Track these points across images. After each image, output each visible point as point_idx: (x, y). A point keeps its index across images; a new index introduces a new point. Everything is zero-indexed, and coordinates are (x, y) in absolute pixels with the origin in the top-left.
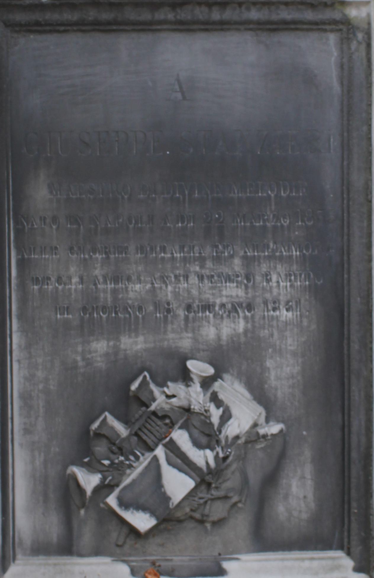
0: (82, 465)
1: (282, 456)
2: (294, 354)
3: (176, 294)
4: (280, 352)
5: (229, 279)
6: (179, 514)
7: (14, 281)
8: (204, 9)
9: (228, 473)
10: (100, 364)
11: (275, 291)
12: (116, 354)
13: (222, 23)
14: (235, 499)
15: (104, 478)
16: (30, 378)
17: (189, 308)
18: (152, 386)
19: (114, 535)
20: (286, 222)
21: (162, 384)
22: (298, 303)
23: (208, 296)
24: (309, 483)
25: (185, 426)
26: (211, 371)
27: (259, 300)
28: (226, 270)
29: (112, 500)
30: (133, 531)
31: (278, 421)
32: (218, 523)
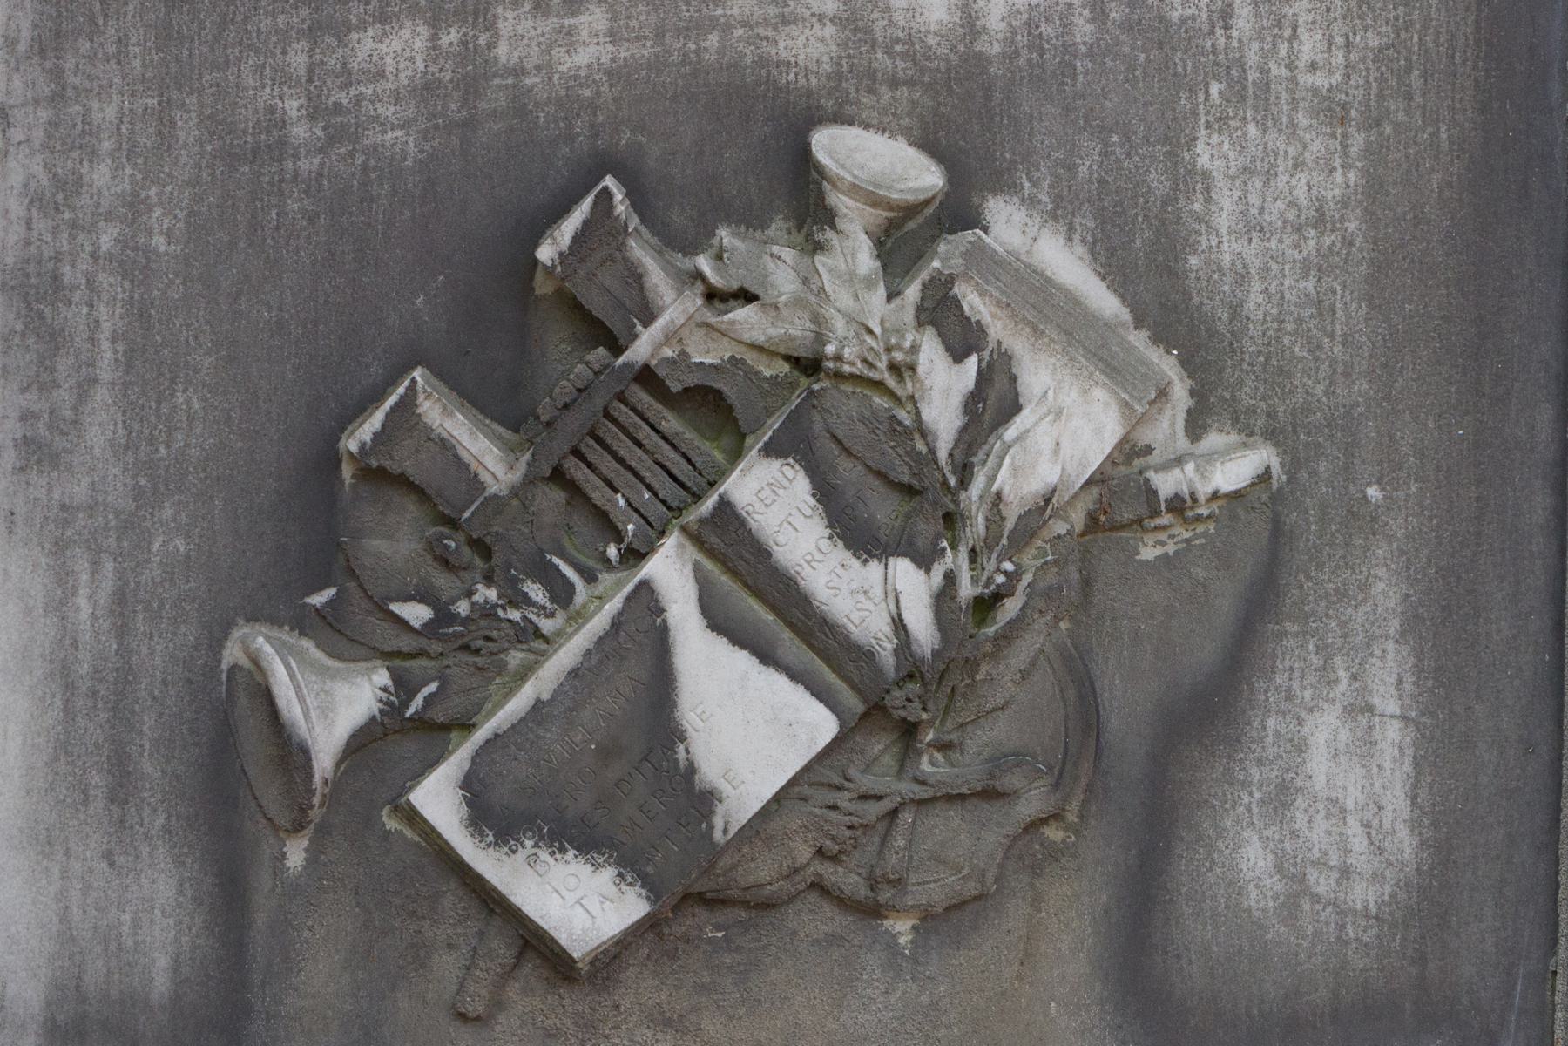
0: (305, 623)
2: (1333, 112)
6: (762, 870)
12: (471, 87)
14: (1032, 803)
15: (404, 686)
18: (641, 252)
19: (447, 966)
24: (1392, 734)
31: (1246, 428)
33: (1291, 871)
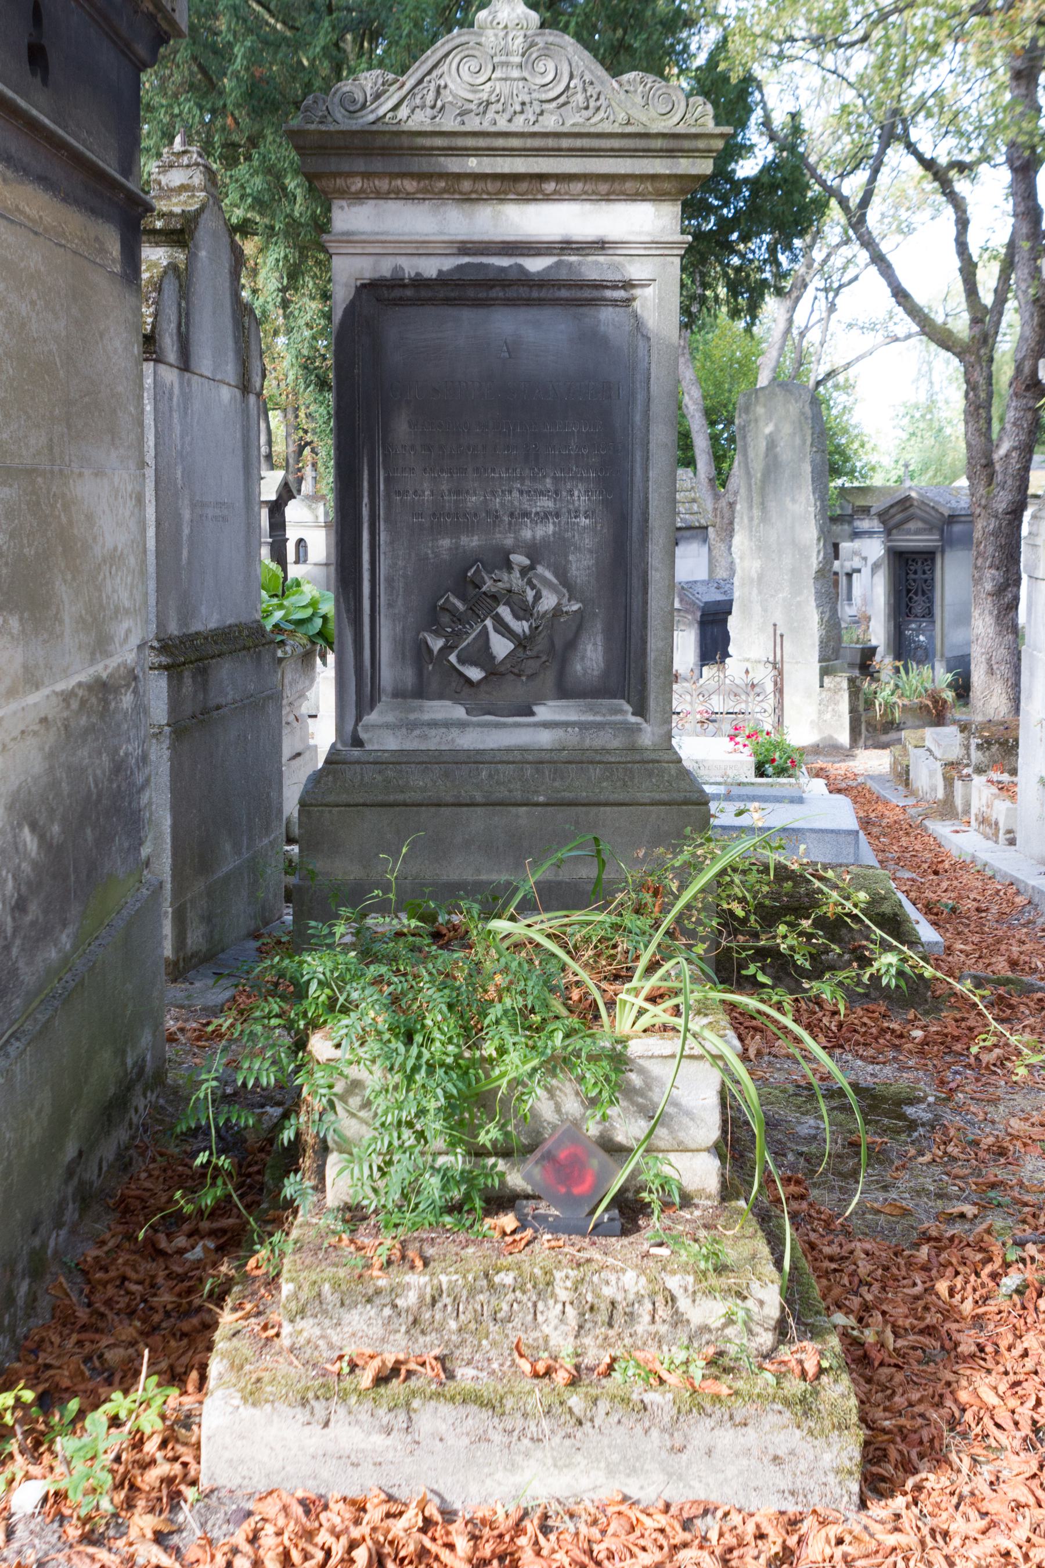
1: (580, 628)
2: (590, 551)
3: (502, 504)
4: (578, 549)
5: (542, 493)
6: (502, 669)
7: (382, 493)
8: (526, 289)
9: (539, 639)
10: (445, 556)
11: (577, 503)
12: (457, 548)
13: (540, 299)
14: (544, 659)
15: (447, 641)
16: (393, 566)
17: (512, 515)
18: (484, 574)
19: (454, 684)
20: (585, 452)
21: (490, 572)
22: (593, 512)
23: (526, 506)
24: (600, 648)
25: (507, 603)
26: (527, 562)
27: (564, 510)
28: (540, 487)
29: (453, 658)
30: (468, 681)
31: (577, 601)
32: (531, 677)
33: (584, 669)
